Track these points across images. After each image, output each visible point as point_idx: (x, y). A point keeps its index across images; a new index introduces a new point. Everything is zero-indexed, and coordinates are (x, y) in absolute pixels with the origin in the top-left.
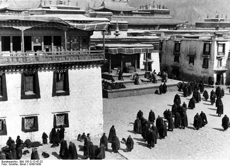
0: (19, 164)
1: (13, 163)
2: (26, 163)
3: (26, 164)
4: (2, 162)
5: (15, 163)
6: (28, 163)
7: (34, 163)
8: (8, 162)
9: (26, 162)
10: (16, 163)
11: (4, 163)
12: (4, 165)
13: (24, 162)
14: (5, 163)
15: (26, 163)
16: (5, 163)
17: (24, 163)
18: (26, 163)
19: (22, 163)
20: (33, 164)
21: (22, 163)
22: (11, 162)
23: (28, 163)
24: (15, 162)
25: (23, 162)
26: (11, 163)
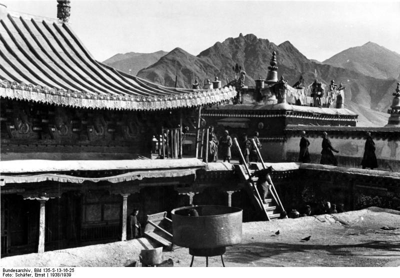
0: (33, 274)
1: (22, 273)
2: (45, 273)
3: (46, 275)
4: (4, 270)
5: (26, 273)
6: (49, 273)
7: (60, 273)
8: (14, 271)
9: (45, 270)
10: (28, 273)
11: (7, 273)
12: (8, 277)
13: (42, 270)
14: (10, 273)
15: (45, 273)
16: (10, 273)
17: (42, 272)
18: (46, 273)
19: (39, 273)
20: (58, 275)
21: (39, 273)
22: (19, 271)
23: (49, 273)
24: (27, 271)
25: (40, 271)
26: (19, 273)
